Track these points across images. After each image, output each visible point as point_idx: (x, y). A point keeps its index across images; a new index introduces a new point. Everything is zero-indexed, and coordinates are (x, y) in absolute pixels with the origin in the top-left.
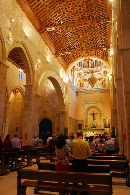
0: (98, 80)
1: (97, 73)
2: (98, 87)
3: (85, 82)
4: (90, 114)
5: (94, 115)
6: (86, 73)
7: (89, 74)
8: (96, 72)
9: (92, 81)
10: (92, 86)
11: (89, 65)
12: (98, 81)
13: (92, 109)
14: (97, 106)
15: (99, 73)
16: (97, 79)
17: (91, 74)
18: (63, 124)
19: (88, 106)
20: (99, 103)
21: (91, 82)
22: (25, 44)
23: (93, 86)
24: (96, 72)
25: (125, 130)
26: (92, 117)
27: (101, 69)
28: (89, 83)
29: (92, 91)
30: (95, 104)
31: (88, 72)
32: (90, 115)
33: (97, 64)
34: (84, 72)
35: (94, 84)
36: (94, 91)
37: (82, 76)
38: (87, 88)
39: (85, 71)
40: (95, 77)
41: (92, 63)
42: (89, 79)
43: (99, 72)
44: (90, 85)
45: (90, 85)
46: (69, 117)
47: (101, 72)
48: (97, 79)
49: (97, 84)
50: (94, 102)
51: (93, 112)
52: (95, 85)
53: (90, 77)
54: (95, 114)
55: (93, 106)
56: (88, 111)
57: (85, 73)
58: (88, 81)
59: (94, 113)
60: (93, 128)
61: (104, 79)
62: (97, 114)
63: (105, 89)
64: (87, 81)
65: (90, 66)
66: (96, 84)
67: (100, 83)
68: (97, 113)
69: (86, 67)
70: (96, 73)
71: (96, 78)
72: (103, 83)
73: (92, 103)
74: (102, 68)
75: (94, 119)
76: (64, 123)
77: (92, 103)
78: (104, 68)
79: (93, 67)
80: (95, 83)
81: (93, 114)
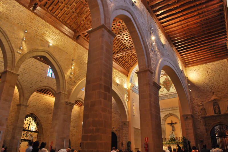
4: (168, 124)
5: (172, 125)
9: (168, 84)
10: (167, 90)
13: (170, 117)
18: (126, 137)
19: (164, 114)
20: (176, 109)
21: (166, 86)
22: (49, 52)
23: (168, 90)
25: (148, 138)
26: (171, 127)
29: (168, 96)
30: (173, 111)
32: (168, 125)
35: (170, 87)
36: (170, 96)
38: (162, 93)
45: (165, 89)
46: (134, 128)
50: (170, 109)
52: (171, 89)
53: (165, 80)
54: (174, 123)
55: (170, 113)
56: (165, 121)
59: (173, 122)
60: (171, 141)
62: (176, 123)
66: (172, 87)
73: (169, 111)
75: (173, 130)
76: (127, 136)
77: (168, 110)
81: (172, 124)
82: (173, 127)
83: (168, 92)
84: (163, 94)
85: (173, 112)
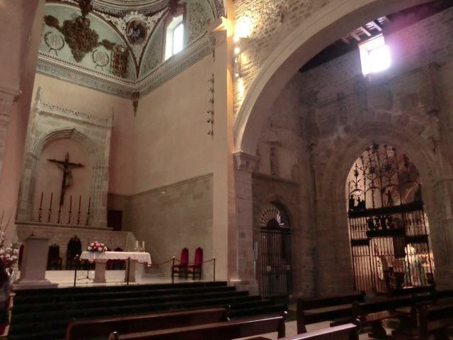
0: (100, 44)
1: (104, 20)
8: (101, 12)
12: (101, 49)
15: (110, 22)
16: (100, 40)
17: (78, 11)
19: (53, 124)
24: (103, 15)
29: (73, 75)
30: (85, 127)
42: (67, 23)
43: (113, 19)
44: (66, 46)
47: (121, 24)
48: (100, 40)
49: (95, 55)
50: (79, 118)
51: (68, 155)
59: (72, 160)
66: (90, 54)
67: (106, 59)
68: (82, 164)
70: (100, 16)
71: (96, 36)
74: (127, 8)
75: (65, 187)
80: (88, 49)
82: (66, 175)
83: (74, 61)
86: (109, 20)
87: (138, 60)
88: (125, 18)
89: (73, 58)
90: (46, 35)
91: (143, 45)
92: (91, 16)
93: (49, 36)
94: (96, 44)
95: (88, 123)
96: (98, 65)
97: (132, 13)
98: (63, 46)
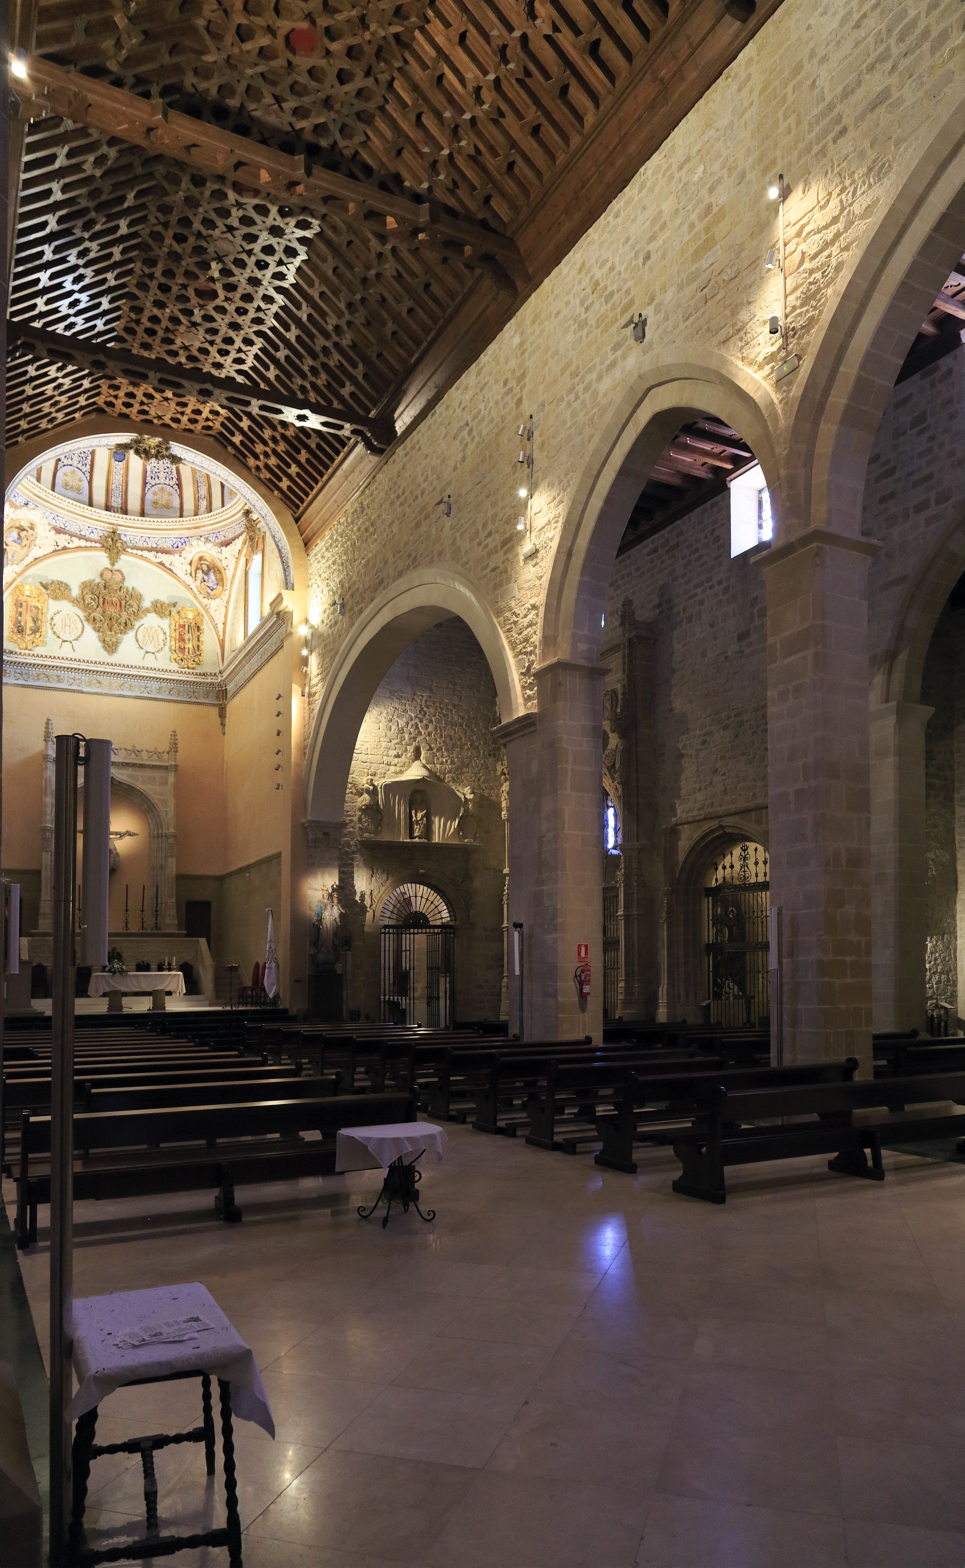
0: (148, 611)
2: (150, 661)
3: (53, 606)
6: (67, 537)
7: (86, 548)
8: (142, 549)
9: (111, 611)
11: (90, 483)
12: (151, 620)
14: (139, 786)
17: (102, 559)
21: (97, 615)
23: (111, 647)
24: (145, 554)
27: (185, 541)
28: (82, 614)
30: (130, 771)
31: (81, 537)
33: (149, 496)
34: (59, 531)
36: (117, 681)
37: (36, 552)
38: (66, 651)
39: (60, 524)
40: (128, 584)
41: (117, 479)
42: (87, 586)
44: (89, 628)
45: (91, 637)
47: (180, 563)
48: (146, 604)
52: (128, 641)
57: (63, 540)
58: (81, 602)
61: (190, 615)
63: (192, 678)
64: (75, 602)
65: (99, 497)
66: (131, 634)
67: (162, 637)
69: (69, 493)
71: (139, 598)
72: (182, 639)
74: (187, 533)
78: (207, 540)
79: (125, 511)
80: (127, 626)
83: (104, 656)
84: (71, 655)
85: (129, 776)
86: (159, 560)
87: (220, 627)
88: (184, 554)
89: (102, 650)
90: (52, 619)
91: (225, 598)
92: (125, 562)
93: (57, 619)
94: (138, 613)
95: (134, 765)
96: (147, 652)
97: (194, 542)
98: (83, 631)
